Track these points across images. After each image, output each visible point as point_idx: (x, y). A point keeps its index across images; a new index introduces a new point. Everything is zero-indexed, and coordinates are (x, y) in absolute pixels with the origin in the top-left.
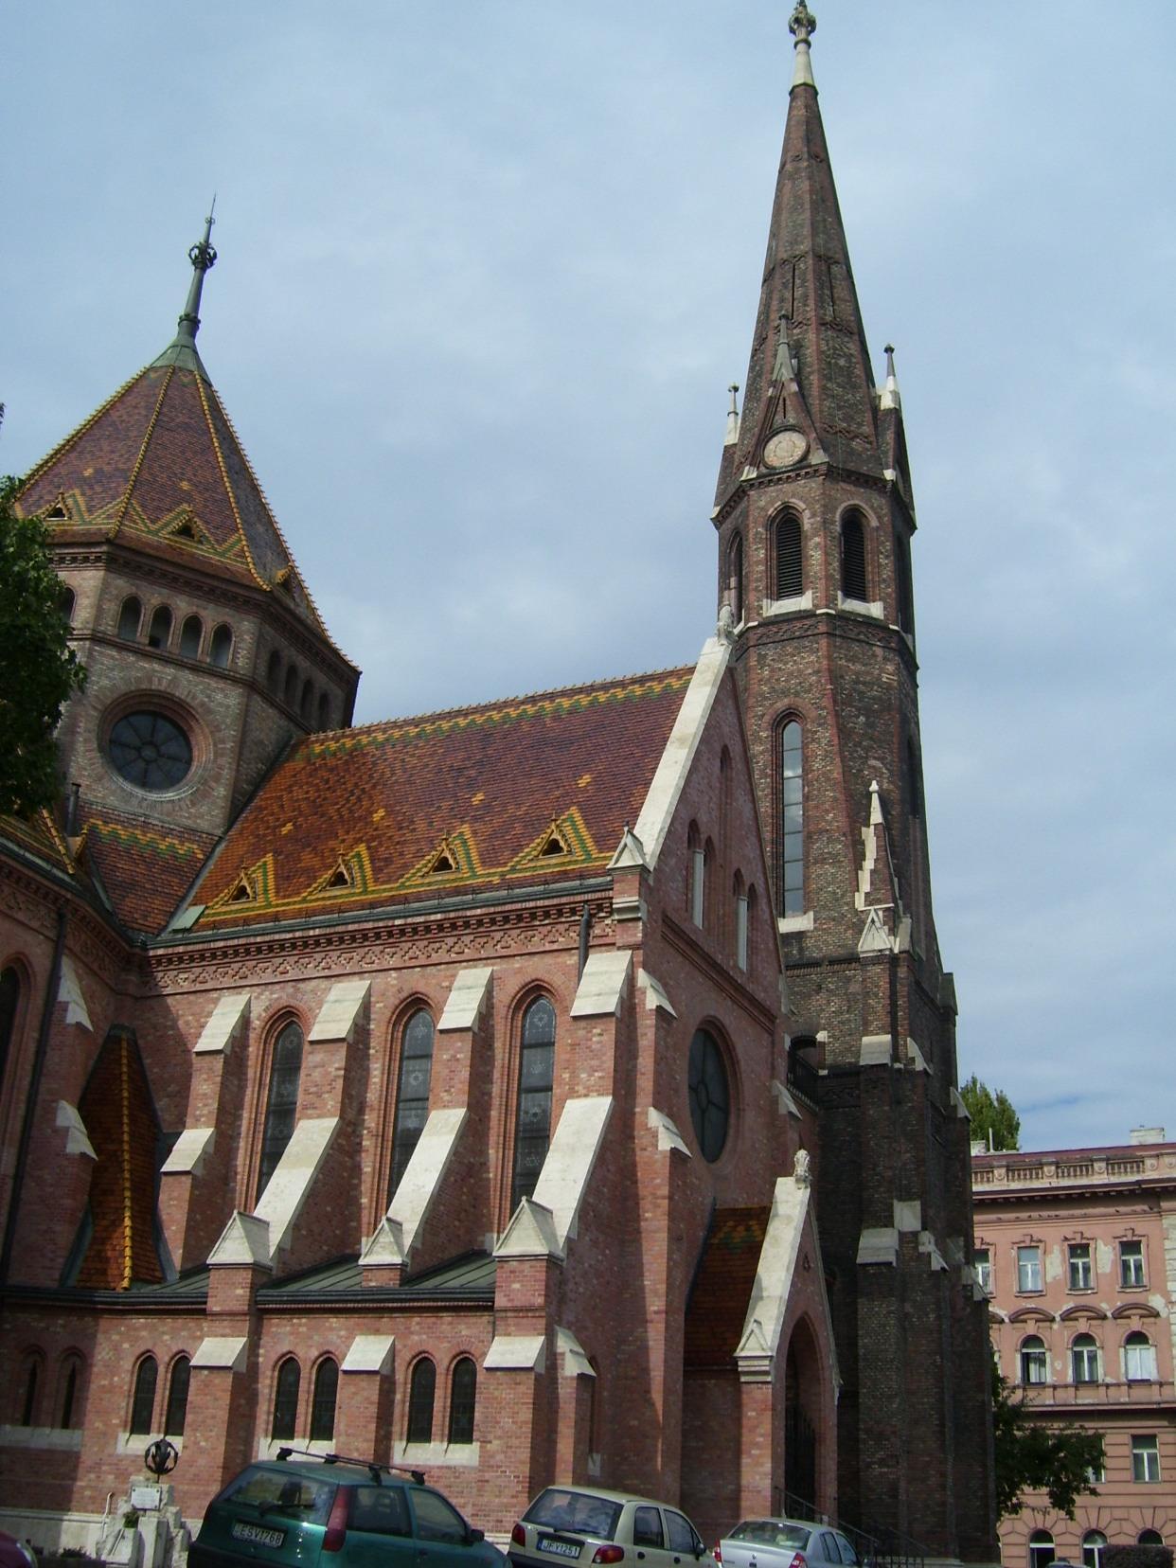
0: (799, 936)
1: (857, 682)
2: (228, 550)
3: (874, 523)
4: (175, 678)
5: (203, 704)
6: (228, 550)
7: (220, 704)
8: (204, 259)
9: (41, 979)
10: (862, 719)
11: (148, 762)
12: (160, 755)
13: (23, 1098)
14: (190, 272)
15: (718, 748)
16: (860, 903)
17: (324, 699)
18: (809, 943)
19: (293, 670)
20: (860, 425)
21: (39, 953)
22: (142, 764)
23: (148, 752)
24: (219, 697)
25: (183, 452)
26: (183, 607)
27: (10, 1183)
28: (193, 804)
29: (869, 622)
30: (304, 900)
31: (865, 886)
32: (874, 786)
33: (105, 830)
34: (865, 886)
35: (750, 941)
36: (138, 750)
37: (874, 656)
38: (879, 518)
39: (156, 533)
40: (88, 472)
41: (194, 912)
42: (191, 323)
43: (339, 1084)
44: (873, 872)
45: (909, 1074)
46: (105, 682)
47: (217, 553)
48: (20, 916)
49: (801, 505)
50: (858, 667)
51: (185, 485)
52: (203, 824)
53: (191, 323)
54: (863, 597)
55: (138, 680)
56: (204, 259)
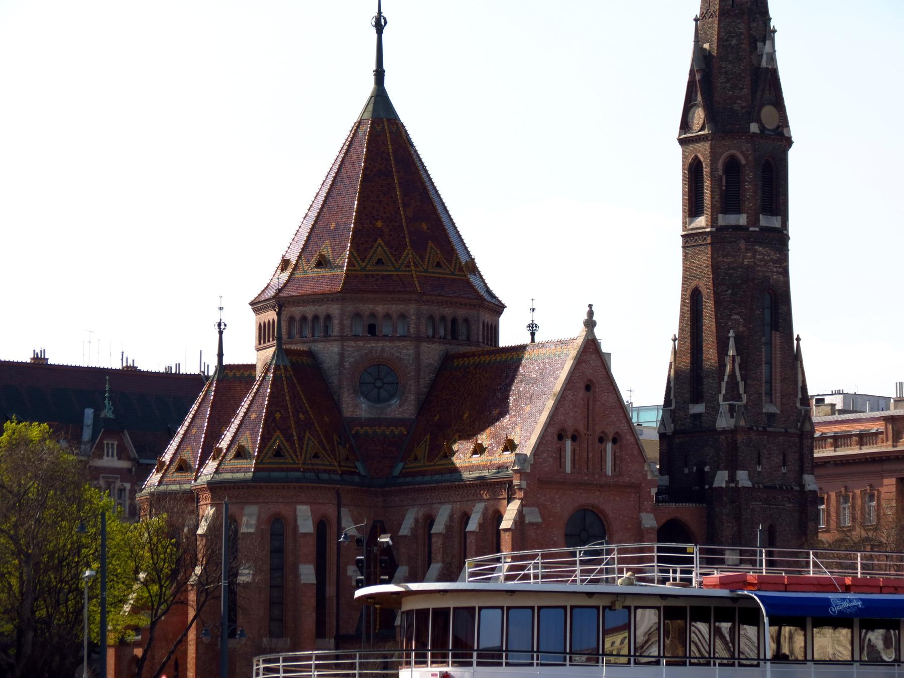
0: (699, 415)
1: (728, 269)
2: (402, 264)
3: (743, 162)
4: (383, 348)
5: (397, 357)
6: (402, 264)
7: (406, 355)
8: (379, 25)
9: (334, 521)
10: (730, 291)
11: (379, 388)
12: (384, 384)
13: (335, 567)
14: (375, 36)
15: (582, 385)
16: (721, 397)
17: (466, 321)
18: (704, 419)
19: (443, 318)
20: (742, 89)
21: (331, 511)
22: (376, 390)
23: (379, 384)
24: (405, 351)
25: (378, 197)
26: (380, 309)
27: (335, 600)
28: (400, 406)
29: (738, 228)
30: (435, 465)
31: (723, 391)
32: (731, 334)
33: (362, 431)
34: (723, 391)
35: (615, 459)
36: (374, 384)
37: (740, 250)
38: (746, 158)
39: (363, 269)
40: (333, 226)
41: (401, 465)
42: (380, 74)
43: (441, 550)
44: (727, 383)
45: (738, 489)
46: (352, 359)
47: (397, 270)
48: (321, 501)
49: (702, 159)
50: (730, 259)
51: (379, 224)
52: (406, 415)
53: (380, 74)
54: (738, 211)
55: (366, 354)
56: (379, 25)
